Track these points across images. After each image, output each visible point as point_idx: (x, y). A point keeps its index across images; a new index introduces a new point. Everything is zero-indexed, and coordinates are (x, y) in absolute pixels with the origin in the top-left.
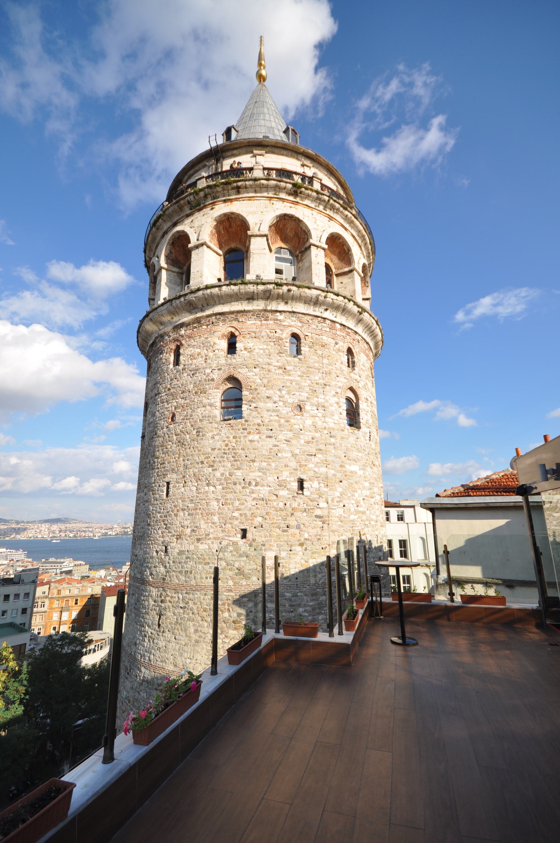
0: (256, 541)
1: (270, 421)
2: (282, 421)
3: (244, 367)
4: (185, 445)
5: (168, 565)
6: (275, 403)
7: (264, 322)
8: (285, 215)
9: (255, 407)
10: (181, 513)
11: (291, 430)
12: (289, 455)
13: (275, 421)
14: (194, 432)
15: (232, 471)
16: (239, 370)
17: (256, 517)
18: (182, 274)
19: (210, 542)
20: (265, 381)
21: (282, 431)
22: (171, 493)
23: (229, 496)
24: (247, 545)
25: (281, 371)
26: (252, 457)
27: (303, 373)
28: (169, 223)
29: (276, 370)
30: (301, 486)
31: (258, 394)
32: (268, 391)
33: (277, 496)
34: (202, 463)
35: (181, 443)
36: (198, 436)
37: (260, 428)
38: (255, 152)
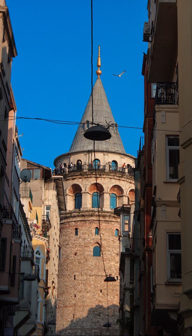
2: (113, 258)
5: (76, 301)
10: (81, 285)
12: (114, 269)
13: (111, 258)
14: (85, 260)
15: (98, 272)
17: (105, 286)
19: (91, 293)
22: (76, 278)
23: (97, 280)
25: (112, 242)
34: (88, 269)
35: (80, 263)
36: (86, 261)
38: (105, 154)
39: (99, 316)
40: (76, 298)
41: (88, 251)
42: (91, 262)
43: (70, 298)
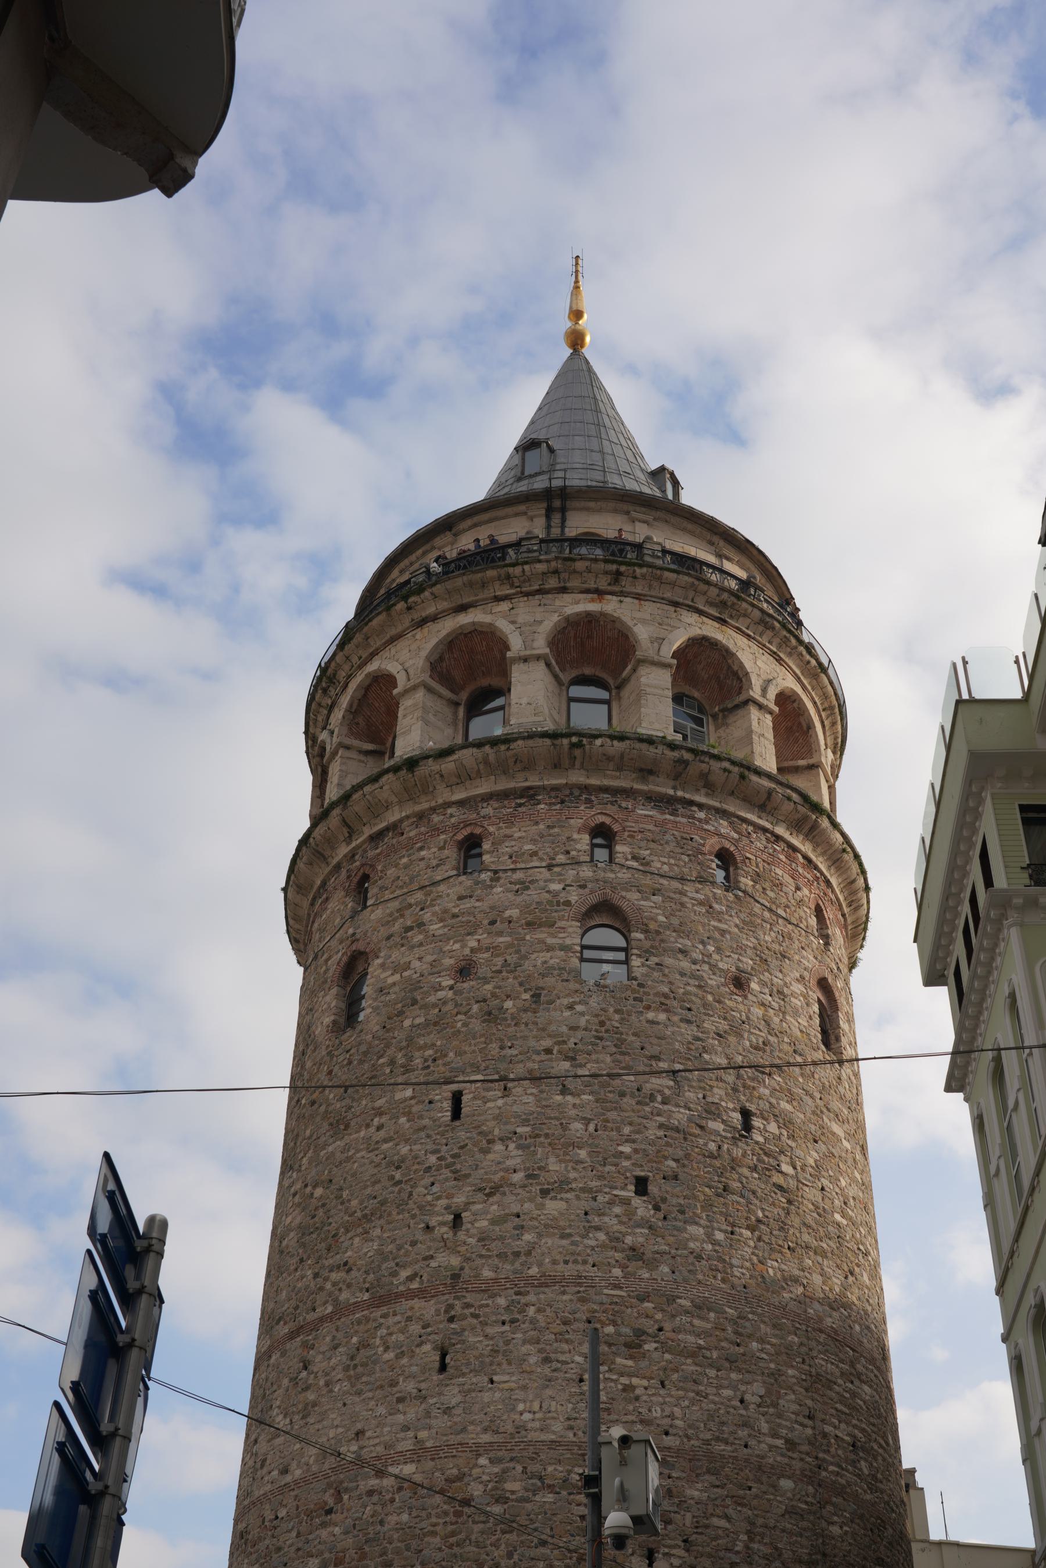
0: (668, 1203)
1: (686, 993)
3: (633, 889)
4: (506, 1019)
6: (694, 962)
7: (668, 817)
8: (705, 638)
9: (657, 964)
10: (499, 1147)
11: (725, 1019)
14: (526, 996)
16: (624, 894)
17: (666, 1158)
18: (457, 704)
20: (675, 921)
21: (708, 1015)
23: (612, 1115)
24: (650, 1207)
26: (655, 1050)
27: (743, 921)
28: (445, 603)
29: (693, 905)
30: (747, 1126)
31: (662, 941)
32: (681, 940)
33: (702, 1127)
34: (548, 1051)
37: (667, 1002)
38: (634, 514)
39: (631, 1357)
40: (461, 1235)
41: (550, 949)
42: (571, 1007)
43: (420, 1236)
